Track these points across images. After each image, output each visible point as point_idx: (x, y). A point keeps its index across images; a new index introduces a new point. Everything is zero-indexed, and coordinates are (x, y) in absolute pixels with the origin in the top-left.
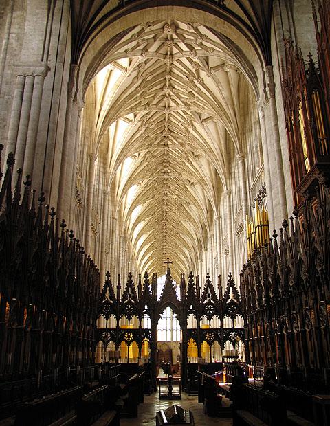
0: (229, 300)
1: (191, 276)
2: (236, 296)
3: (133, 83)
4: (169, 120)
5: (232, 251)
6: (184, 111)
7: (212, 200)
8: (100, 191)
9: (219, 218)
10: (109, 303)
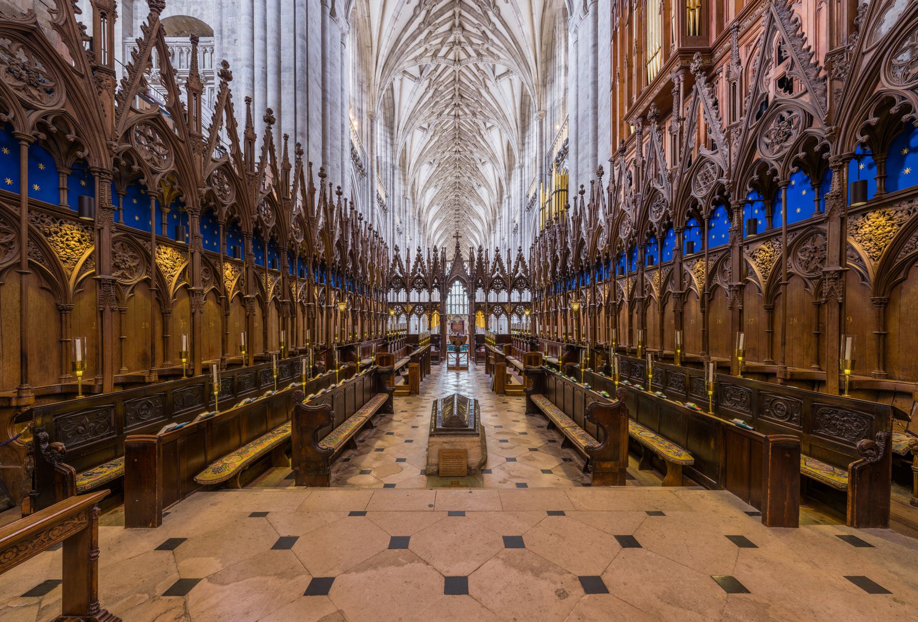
0: (517, 275)
1: (480, 250)
2: (525, 271)
3: (415, 16)
4: (459, 80)
5: (521, 228)
6: (476, 66)
7: (503, 178)
8: (389, 165)
9: (509, 197)
10: (399, 277)
